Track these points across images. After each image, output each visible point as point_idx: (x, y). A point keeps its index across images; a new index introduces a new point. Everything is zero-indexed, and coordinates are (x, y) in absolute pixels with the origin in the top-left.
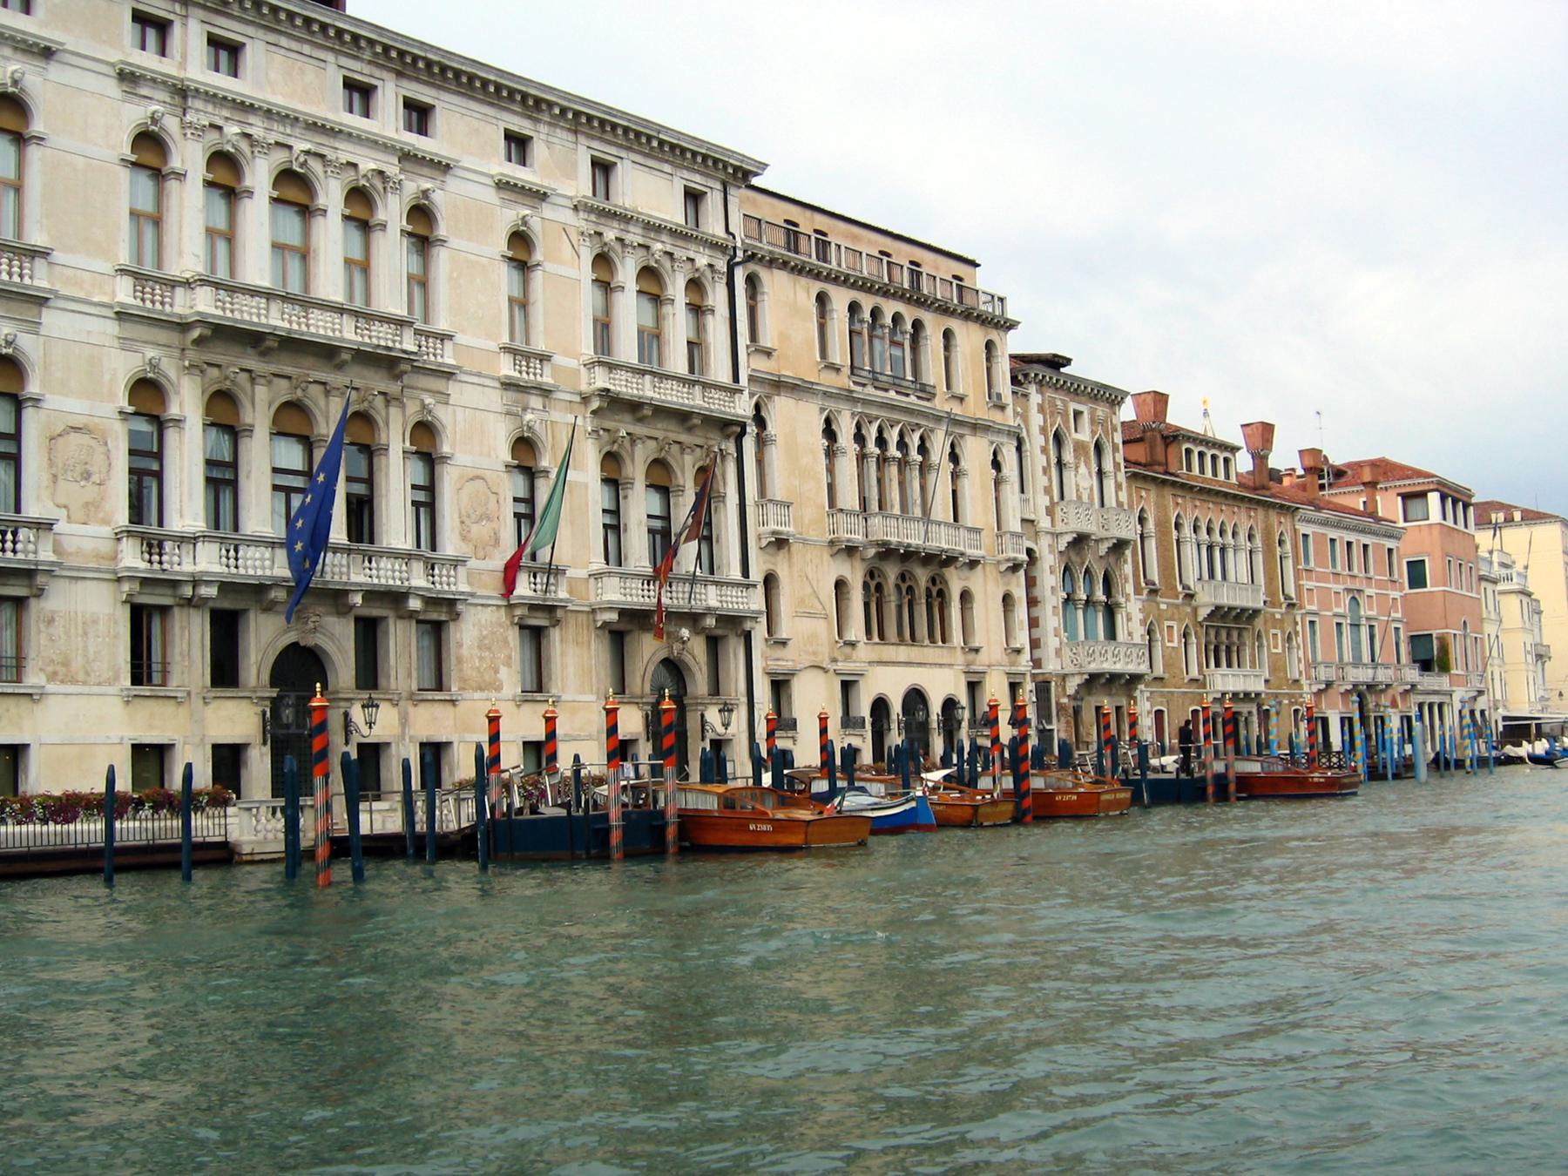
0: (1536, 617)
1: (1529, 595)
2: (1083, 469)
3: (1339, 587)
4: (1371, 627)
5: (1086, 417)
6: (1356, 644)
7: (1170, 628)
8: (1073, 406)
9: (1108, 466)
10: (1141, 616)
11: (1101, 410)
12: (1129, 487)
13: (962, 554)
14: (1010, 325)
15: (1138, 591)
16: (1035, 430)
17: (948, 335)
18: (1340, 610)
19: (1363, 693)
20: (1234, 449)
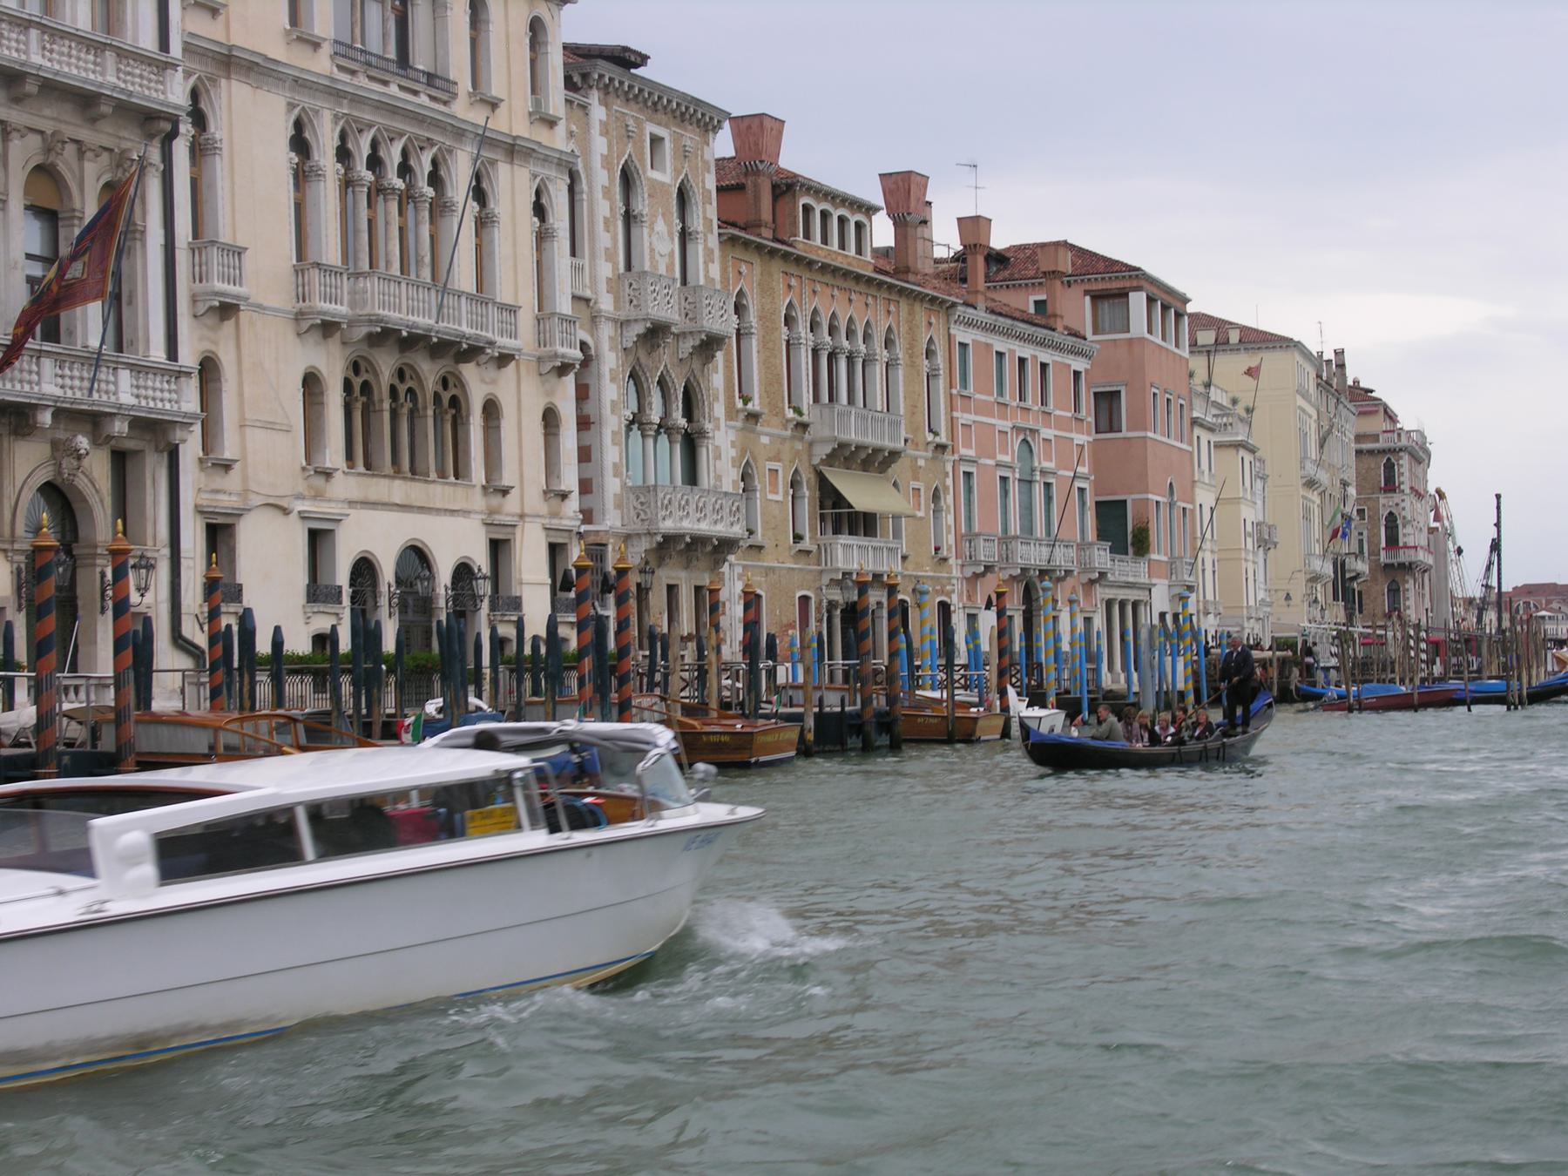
1: (1252, 451)
3: (1005, 425)
4: (1048, 485)
6: (1027, 509)
7: (774, 472)
8: (651, 128)
9: (696, 223)
10: (733, 453)
11: (690, 137)
12: (723, 257)
13: (491, 343)
15: (731, 413)
16: (597, 162)
18: (1007, 459)
19: (1030, 587)
20: (870, 210)
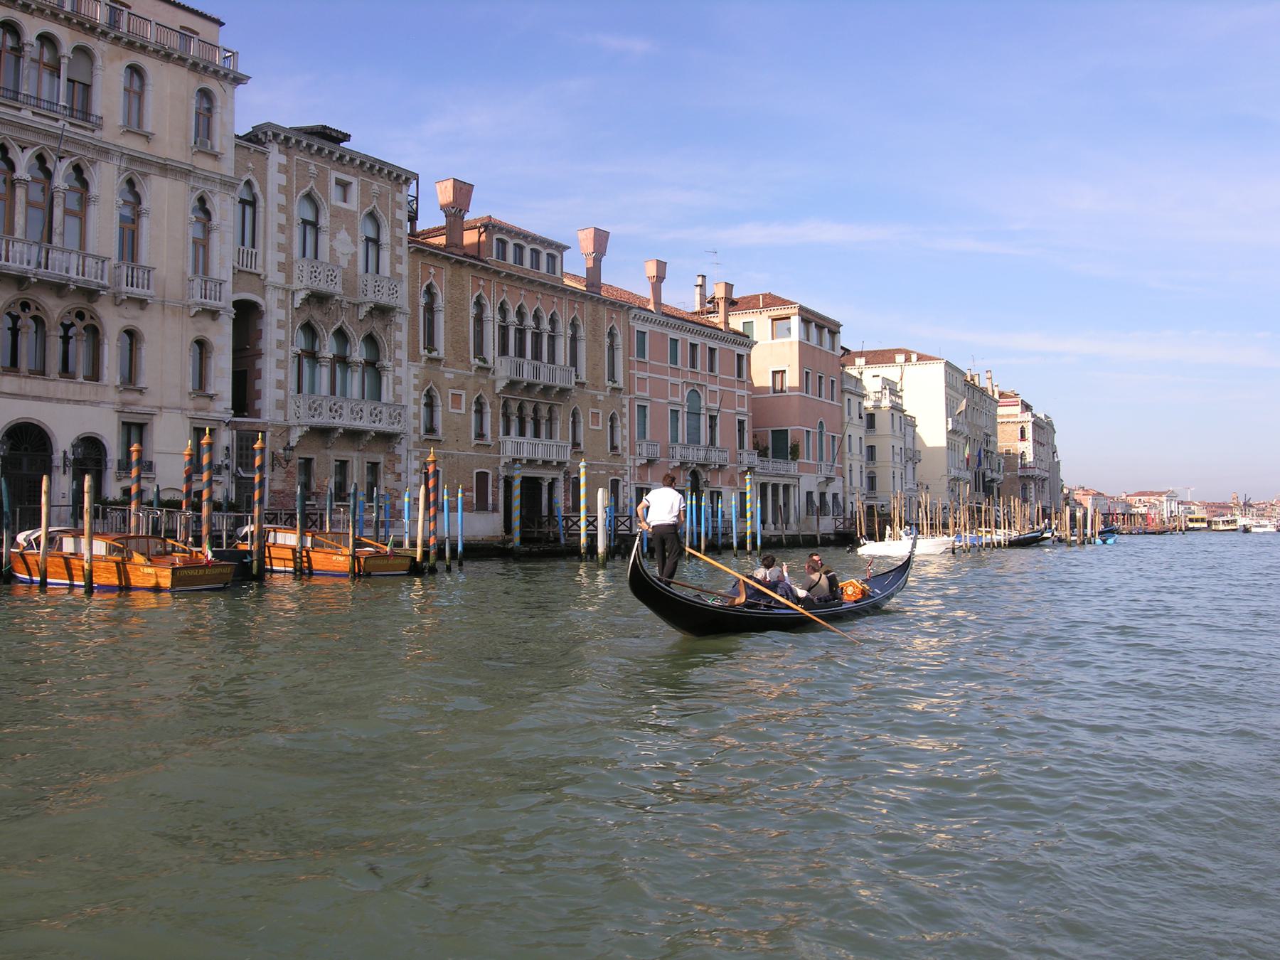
0: (909, 429)
2: (343, 235)
3: (679, 381)
5: (354, 191)
8: (334, 175)
14: (238, 80)
15: (414, 357)
16: (272, 188)
17: (135, 70)
18: (679, 400)
